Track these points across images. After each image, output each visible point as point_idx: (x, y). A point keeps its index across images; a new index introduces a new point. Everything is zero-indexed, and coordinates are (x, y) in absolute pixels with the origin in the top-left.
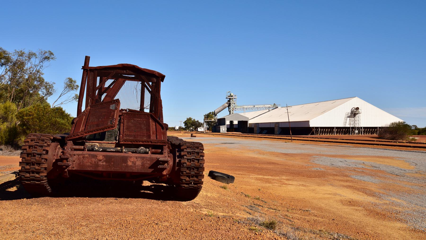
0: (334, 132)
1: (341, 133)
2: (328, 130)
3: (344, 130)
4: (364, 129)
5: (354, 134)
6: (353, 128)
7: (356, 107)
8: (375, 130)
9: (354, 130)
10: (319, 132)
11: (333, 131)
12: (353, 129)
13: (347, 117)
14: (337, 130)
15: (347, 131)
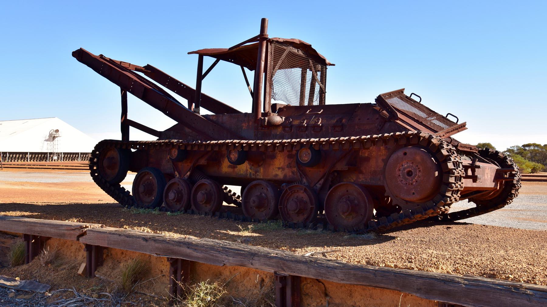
0: (27, 158)
1: (33, 159)
2: (19, 157)
3: (40, 156)
4: (64, 155)
5: (52, 161)
6: (51, 153)
7: (55, 129)
8: (75, 156)
9: (52, 156)
10: (7, 158)
11: (25, 157)
12: (50, 155)
13: (45, 141)
14: (31, 155)
15: (44, 156)
